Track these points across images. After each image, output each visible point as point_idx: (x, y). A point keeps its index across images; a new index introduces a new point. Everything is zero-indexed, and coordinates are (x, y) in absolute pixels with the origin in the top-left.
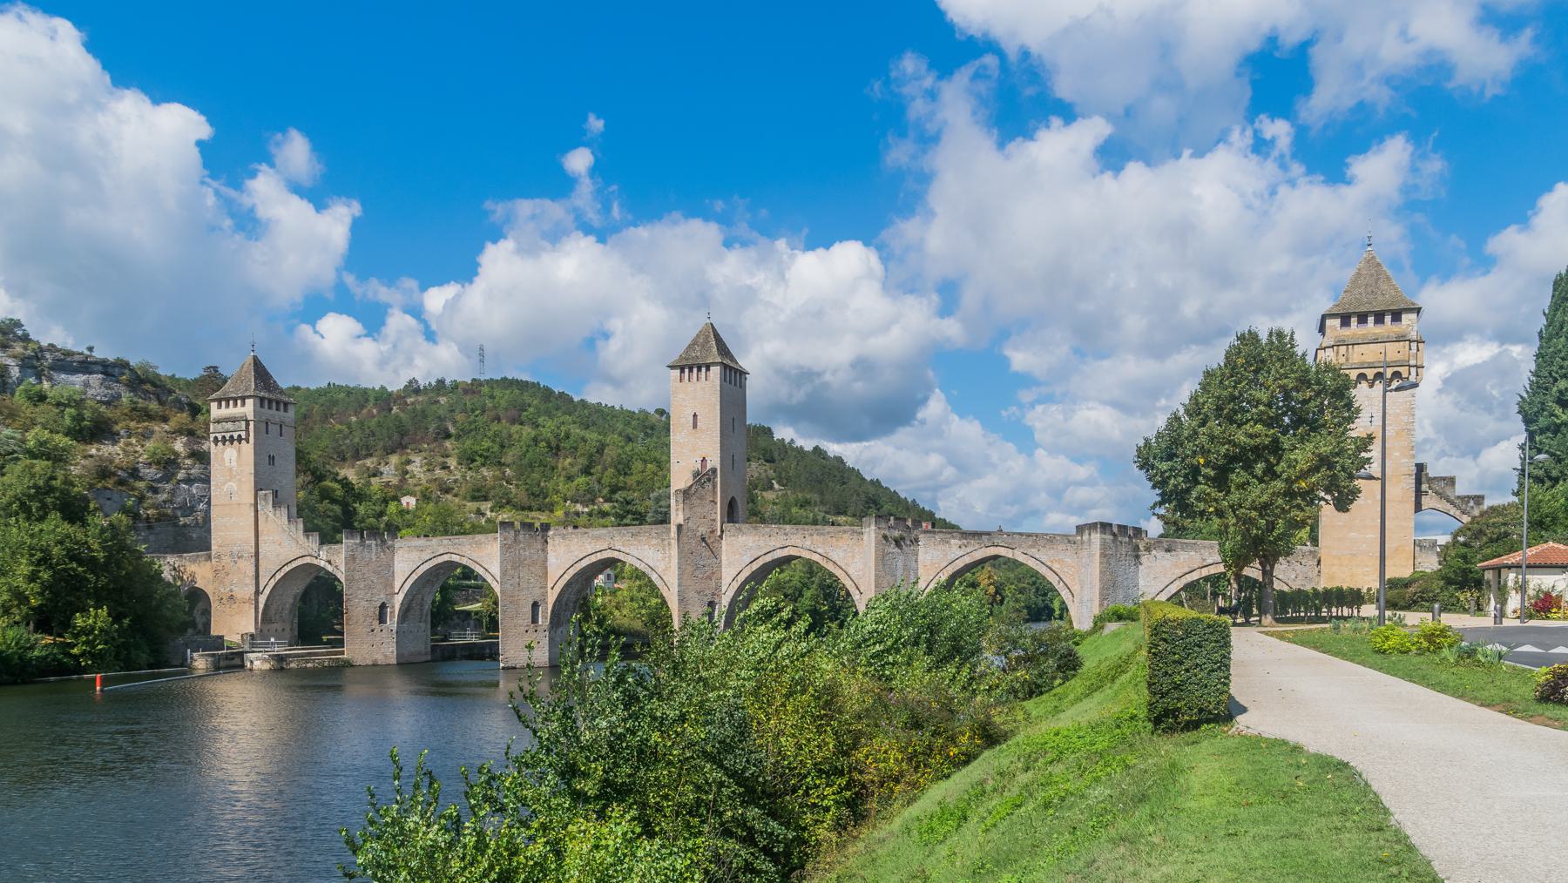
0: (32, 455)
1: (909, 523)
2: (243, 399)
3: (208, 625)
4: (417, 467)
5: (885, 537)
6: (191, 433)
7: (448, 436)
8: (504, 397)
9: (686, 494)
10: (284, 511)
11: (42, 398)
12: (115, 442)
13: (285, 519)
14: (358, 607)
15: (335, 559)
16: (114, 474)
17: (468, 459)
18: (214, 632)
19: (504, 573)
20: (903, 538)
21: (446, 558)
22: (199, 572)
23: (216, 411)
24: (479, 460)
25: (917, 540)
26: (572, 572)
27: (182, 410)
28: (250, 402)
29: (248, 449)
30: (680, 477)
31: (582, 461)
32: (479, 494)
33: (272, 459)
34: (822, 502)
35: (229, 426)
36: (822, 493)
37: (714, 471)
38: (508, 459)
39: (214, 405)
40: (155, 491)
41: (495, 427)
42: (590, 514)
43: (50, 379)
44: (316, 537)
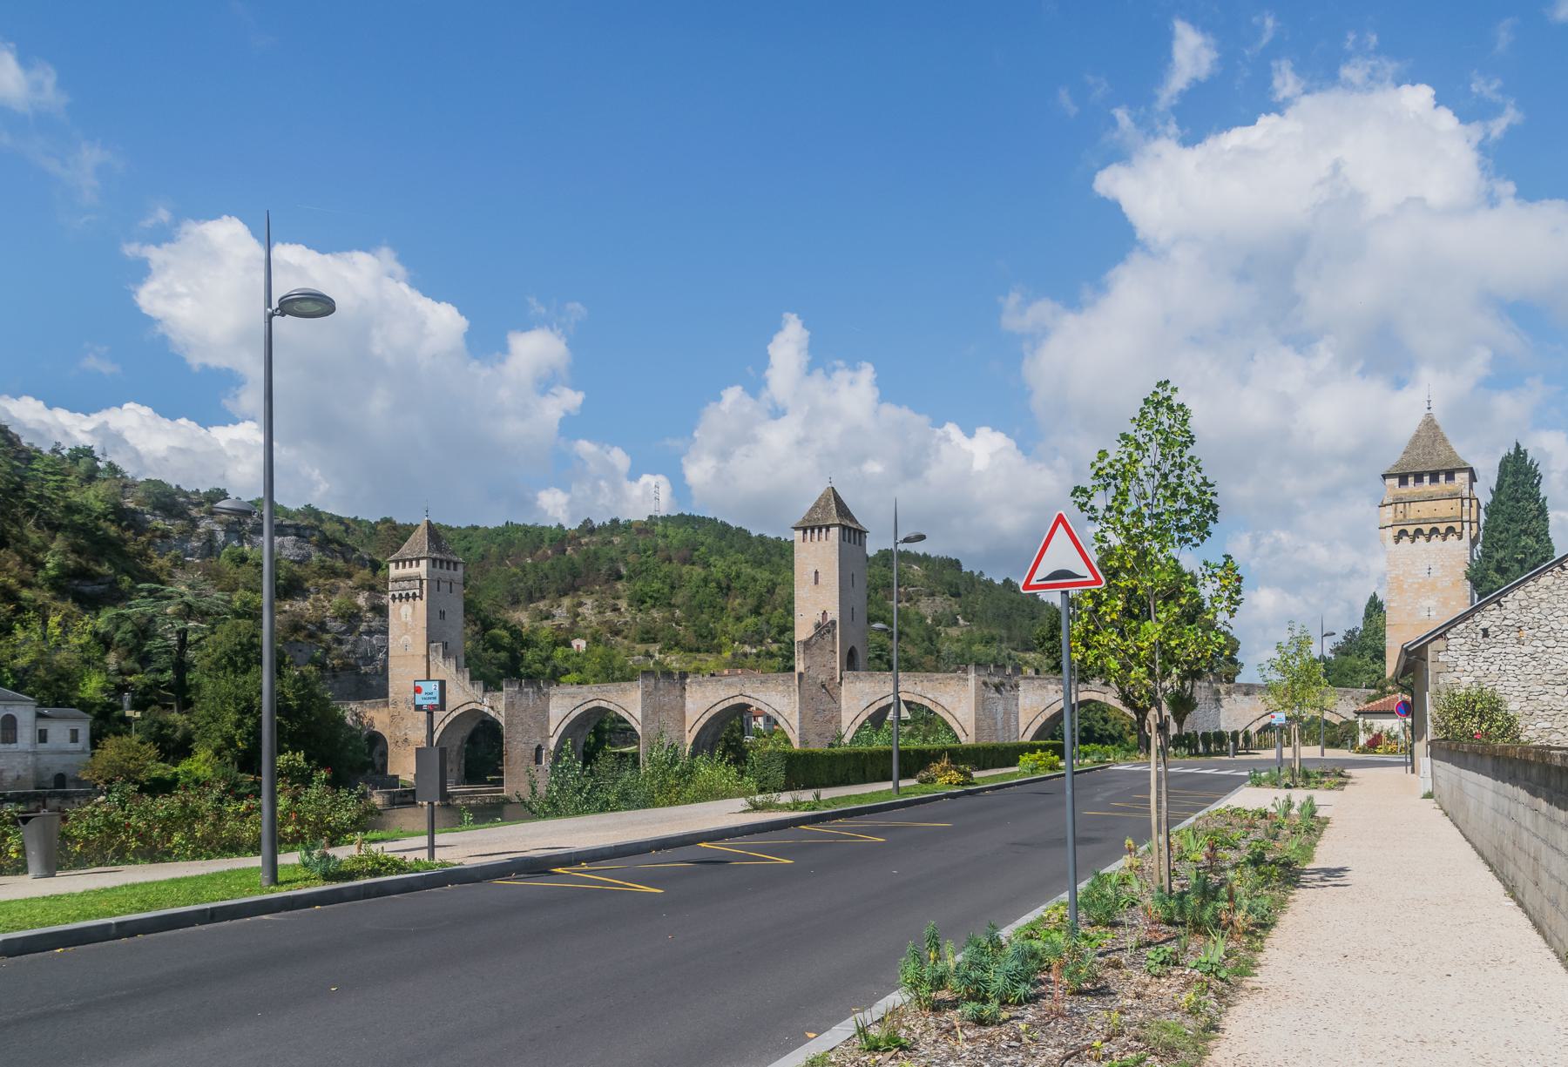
0: (238, 615)
1: (1009, 671)
2: (418, 560)
3: (385, 765)
4: (588, 610)
5: (985, 684)
6: (372, 588)
7: (620, 577)
8: (677, 535)
9: (807, 644)
10: (453, 661)
11: (243, 559)
12: (305, 598)
13: (453, 669)
14: (517, 748)
15: (495, 705)
16: (304, 628)
17: (639, 601)
18: (390, 773)
19: (645, 717)
20: (1003, 684)
21: (595, 704)
22: (378, 718)
23: (394, 571)
24: (650, 602)
25: (1017, 686)
26: (707, 716)
27: (364, 567)
28: (423, 563)
29: (421, 605)
30: (803, 630)
31: (751, 602)
32: (648, 636)
33: (442, 614)
34: (1010, 639)
35: (405, 584)
36: (1009, 629)
37: (833, 623)
38: (678, 599)
39: (392, 566)
40: (340, 642)
41: (666, 568)
42: (758, 655)
43: (250, 542)
44: (481, 684)
